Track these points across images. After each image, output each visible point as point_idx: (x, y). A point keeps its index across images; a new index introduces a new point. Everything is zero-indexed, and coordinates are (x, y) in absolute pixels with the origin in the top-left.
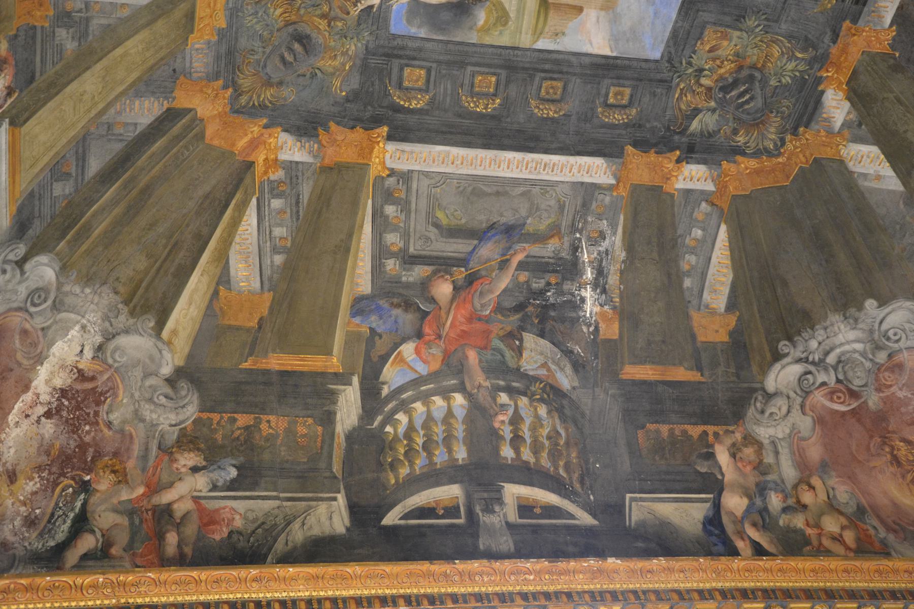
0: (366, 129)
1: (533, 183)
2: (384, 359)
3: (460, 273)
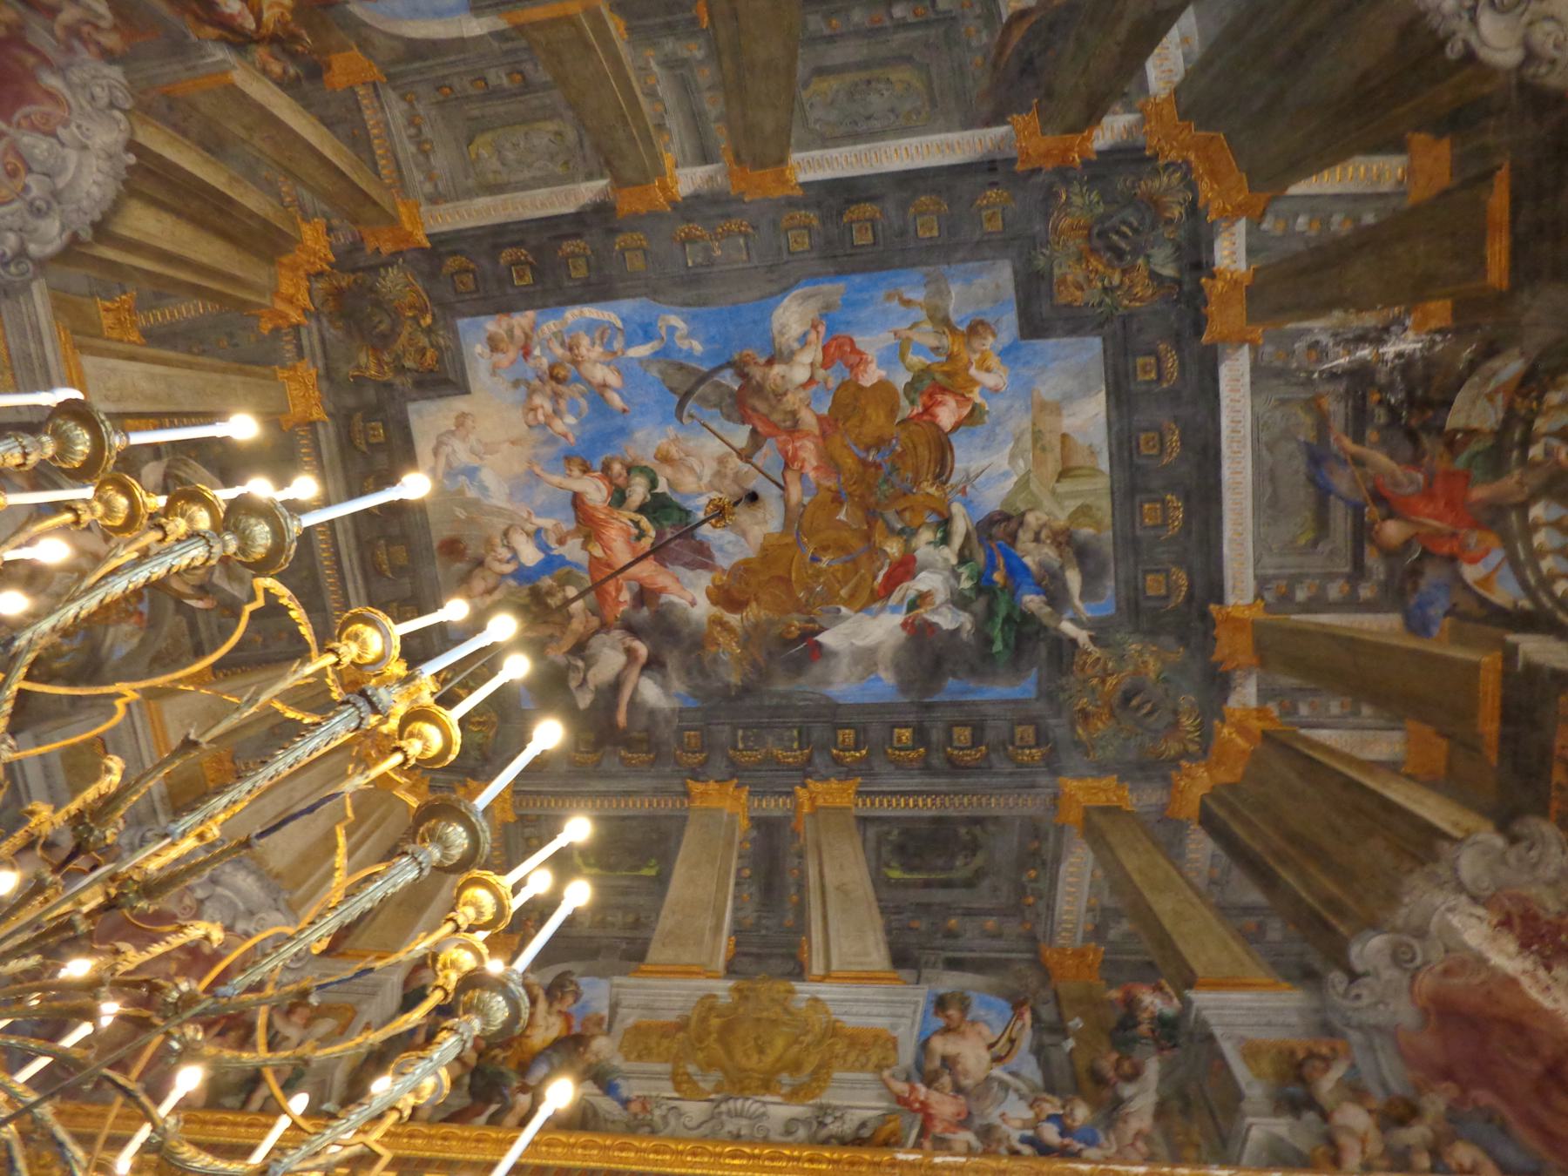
0: (1214, 626)
1: (1256, 441)
2: (1484, 602)
3: (1372, 512)
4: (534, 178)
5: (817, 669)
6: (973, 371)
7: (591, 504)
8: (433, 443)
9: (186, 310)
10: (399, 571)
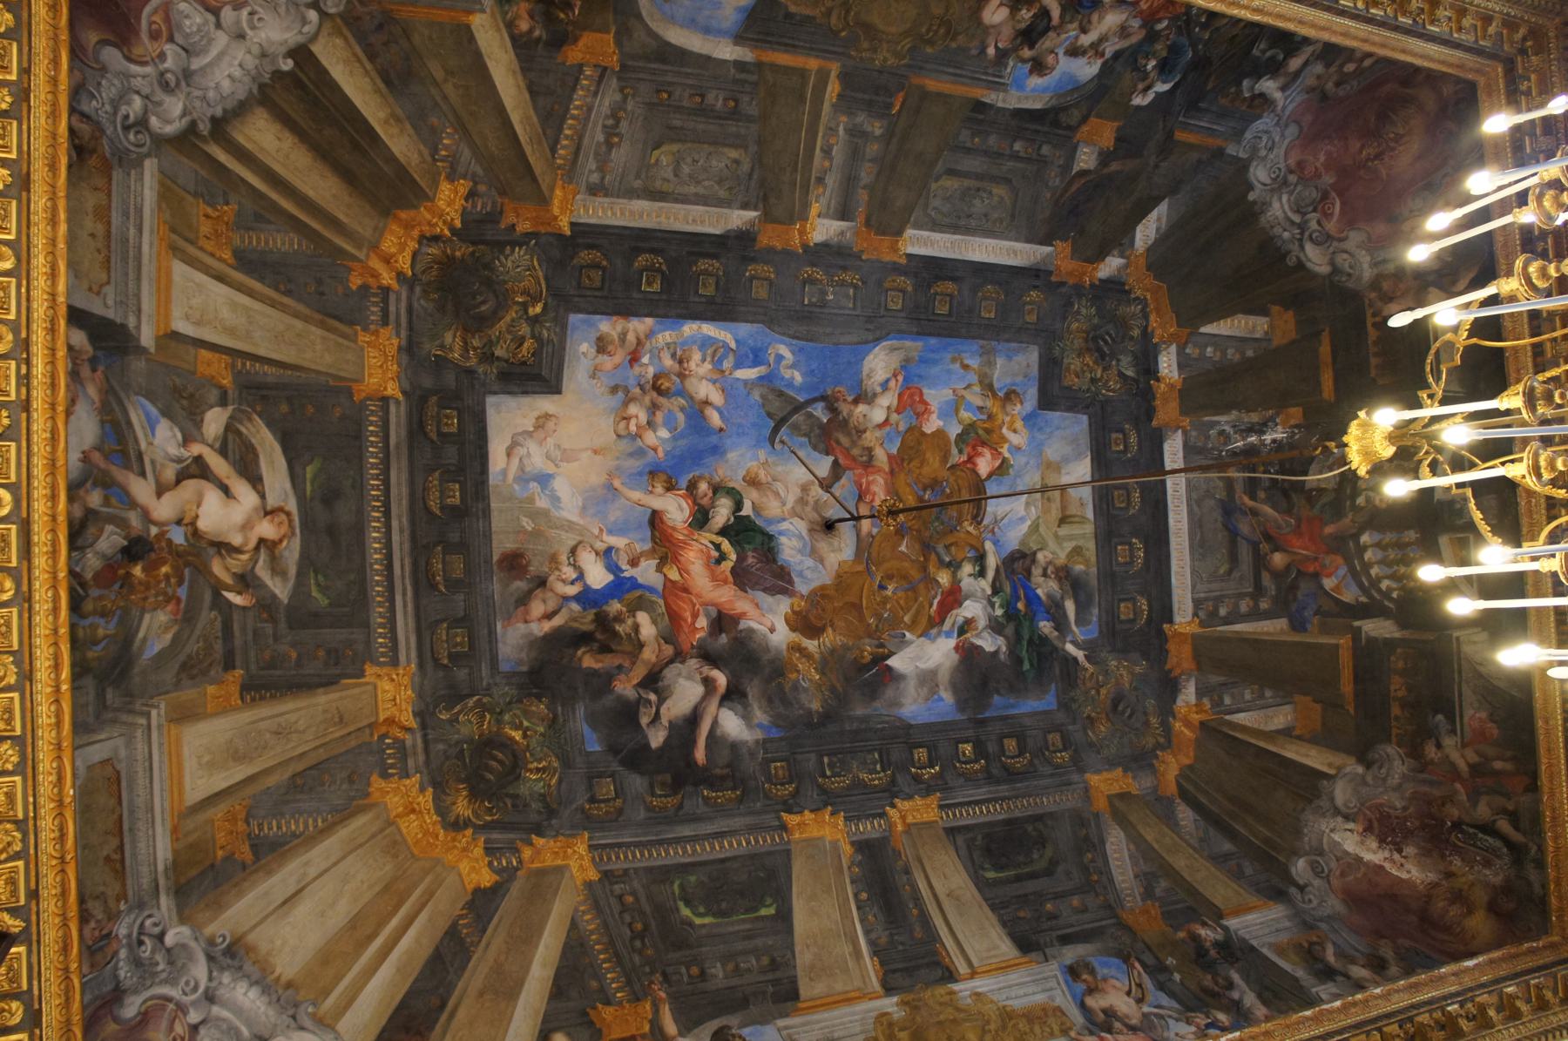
2: (1338, 602)
4: (696, 194)
5: (889, 693)
6: (1004, 430)
7: (670, 523)
8: (508, 442)
9: (282, 242)
10: (454, 585)
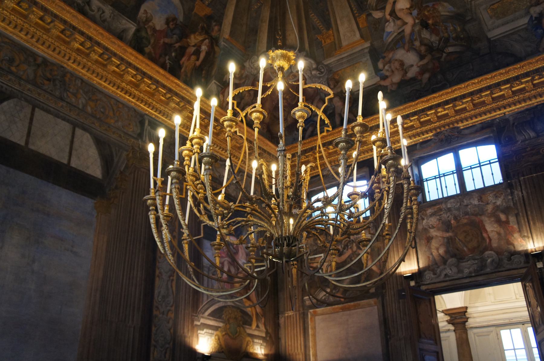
9: (315, 19)
